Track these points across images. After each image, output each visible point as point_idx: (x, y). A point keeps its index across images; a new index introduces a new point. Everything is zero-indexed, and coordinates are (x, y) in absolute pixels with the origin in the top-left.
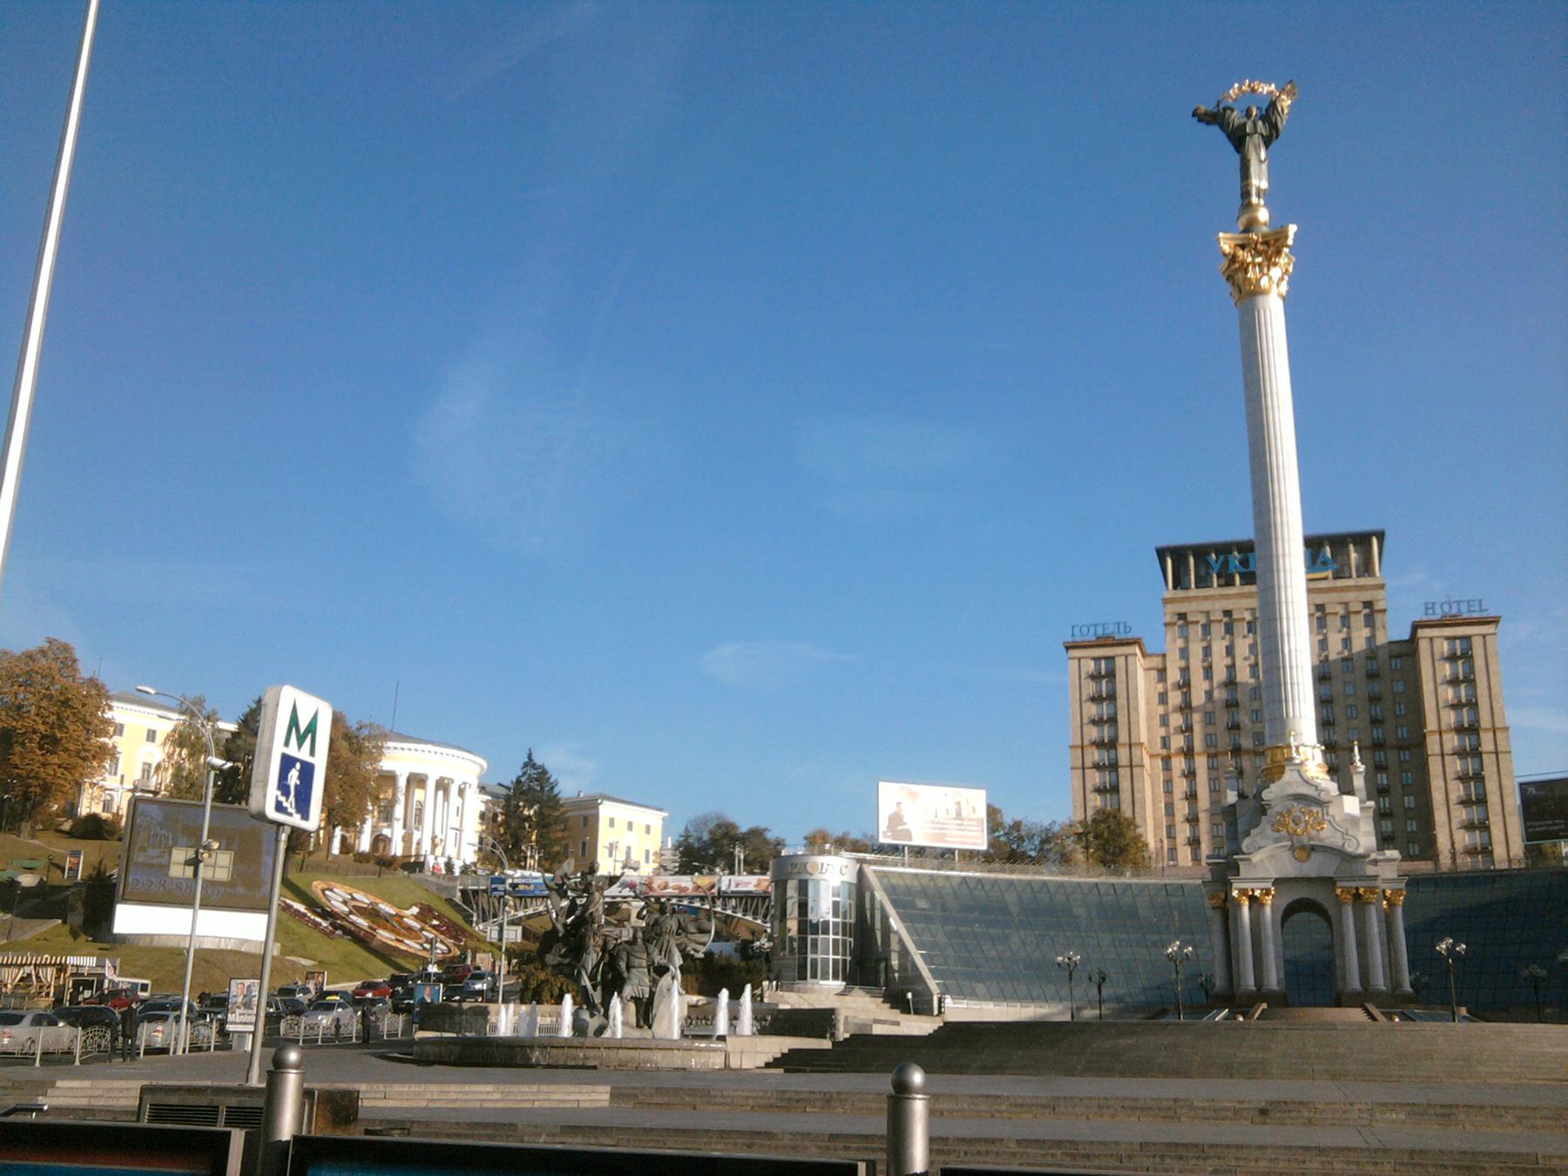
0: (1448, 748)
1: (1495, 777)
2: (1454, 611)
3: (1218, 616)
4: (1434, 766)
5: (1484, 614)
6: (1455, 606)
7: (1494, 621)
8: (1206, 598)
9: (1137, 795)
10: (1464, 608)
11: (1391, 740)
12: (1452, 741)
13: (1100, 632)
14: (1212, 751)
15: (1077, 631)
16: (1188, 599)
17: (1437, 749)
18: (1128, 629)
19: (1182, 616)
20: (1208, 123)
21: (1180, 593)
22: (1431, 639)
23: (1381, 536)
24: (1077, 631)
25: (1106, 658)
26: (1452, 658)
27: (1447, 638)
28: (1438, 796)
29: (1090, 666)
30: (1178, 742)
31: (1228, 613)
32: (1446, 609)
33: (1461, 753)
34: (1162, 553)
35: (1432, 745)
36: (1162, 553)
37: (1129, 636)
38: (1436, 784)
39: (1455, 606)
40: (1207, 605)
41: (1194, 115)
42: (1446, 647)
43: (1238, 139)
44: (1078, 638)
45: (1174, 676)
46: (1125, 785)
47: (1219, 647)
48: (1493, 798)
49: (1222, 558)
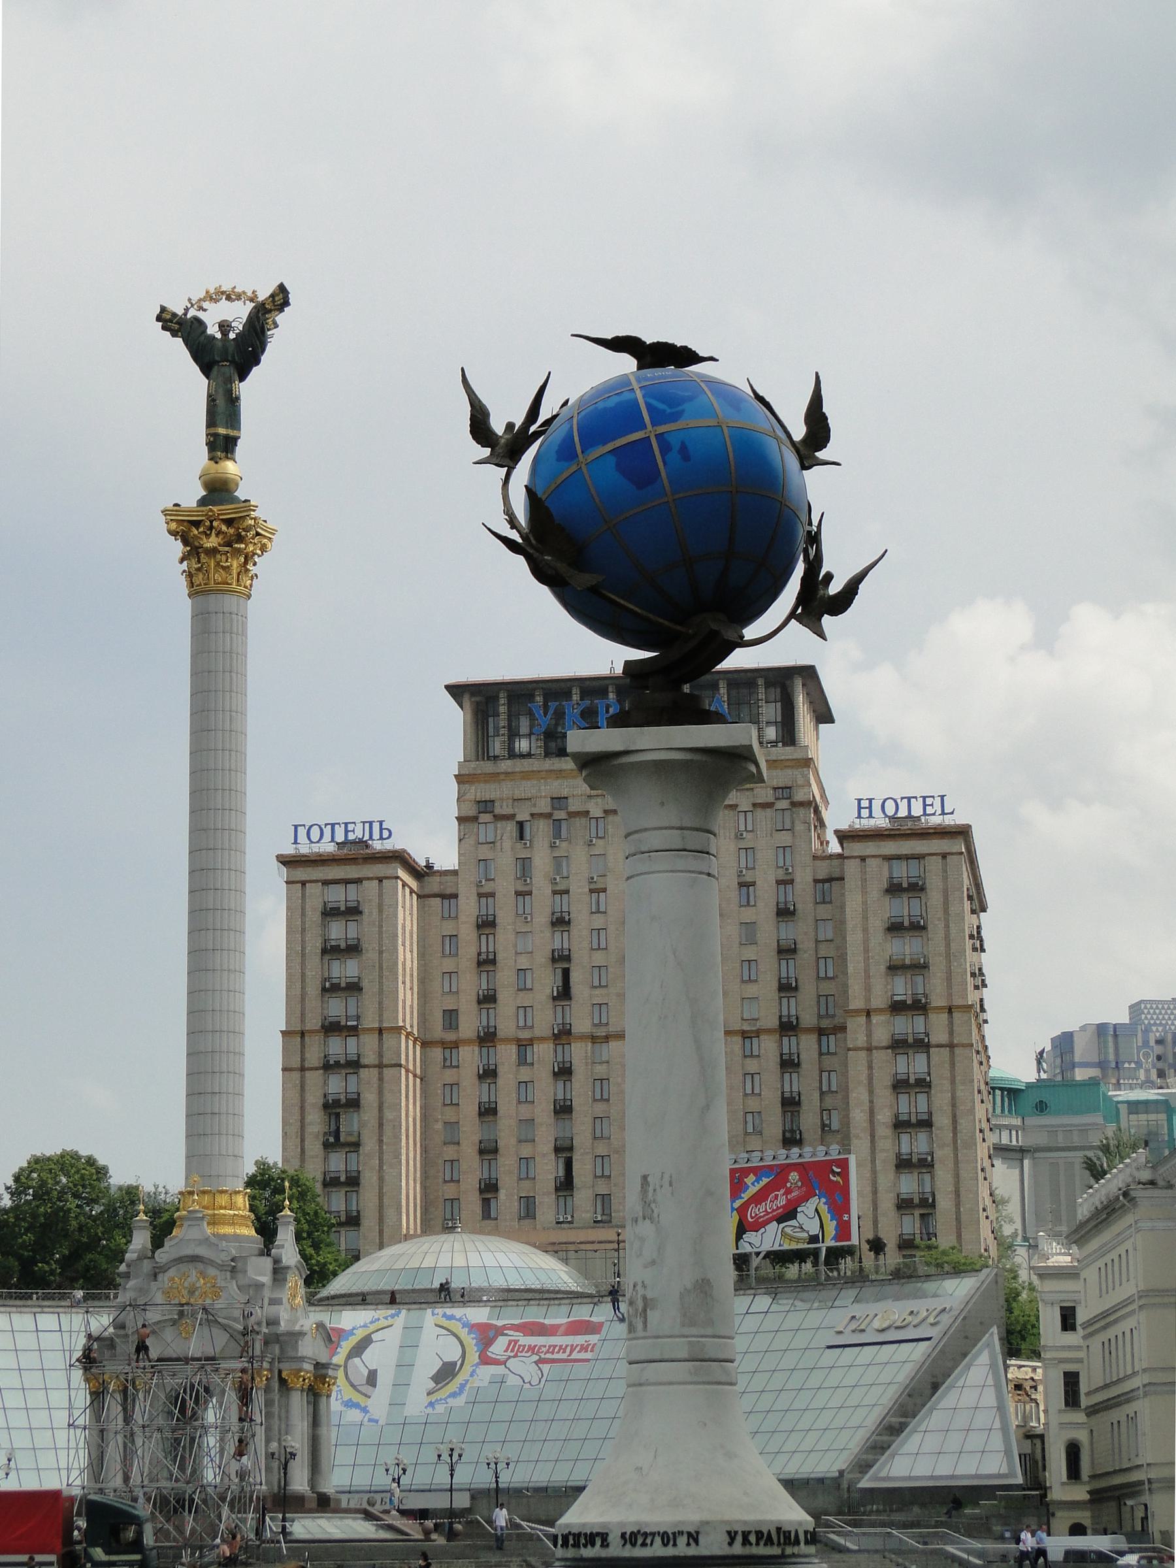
0: (882, 1035)
1: (947, 1085)
2: (903, 813)
3: (544, 806)
4: (857, 1064)
5: (949, 821)
6: (903, 805)
7: (963, 833)
8: (526, 775)
9: (389, 1115)
10: (917, 810)
11: (808, 1019)
12: (884, 1029)
13: (340, 838)
14: (525, 1035)
15: (302, 832)
16: (494, 777)
17: (861, 1040)
18: (386, 833)
19: (485, 806)
20: (174, 334)
21: (488, 767)
22: (863, 859)
23: (808, 673)
24: (302, 832)
25: (347, 882)
26: (894, 889)
27: (889, 858)
28: (859, 1116)
29: (316, 896)
30: (469, 1026)
31: (559, 801)
32: (890, 808)
33: (899, 1045)
34: (456, 691)
35: (857, 1031)
36: (456, 691)
37: (388, 845)
38: (859, 1095)
39: (903, 805)
40: (526, 788)
41: (159, 319)
42: (879, 874)
43: (206, 369)
44: (305, 849)
45: (468, 907)
46: (369, 1098)
47: (541, 860)
48: (942, 1120)
49: (553, 705)
